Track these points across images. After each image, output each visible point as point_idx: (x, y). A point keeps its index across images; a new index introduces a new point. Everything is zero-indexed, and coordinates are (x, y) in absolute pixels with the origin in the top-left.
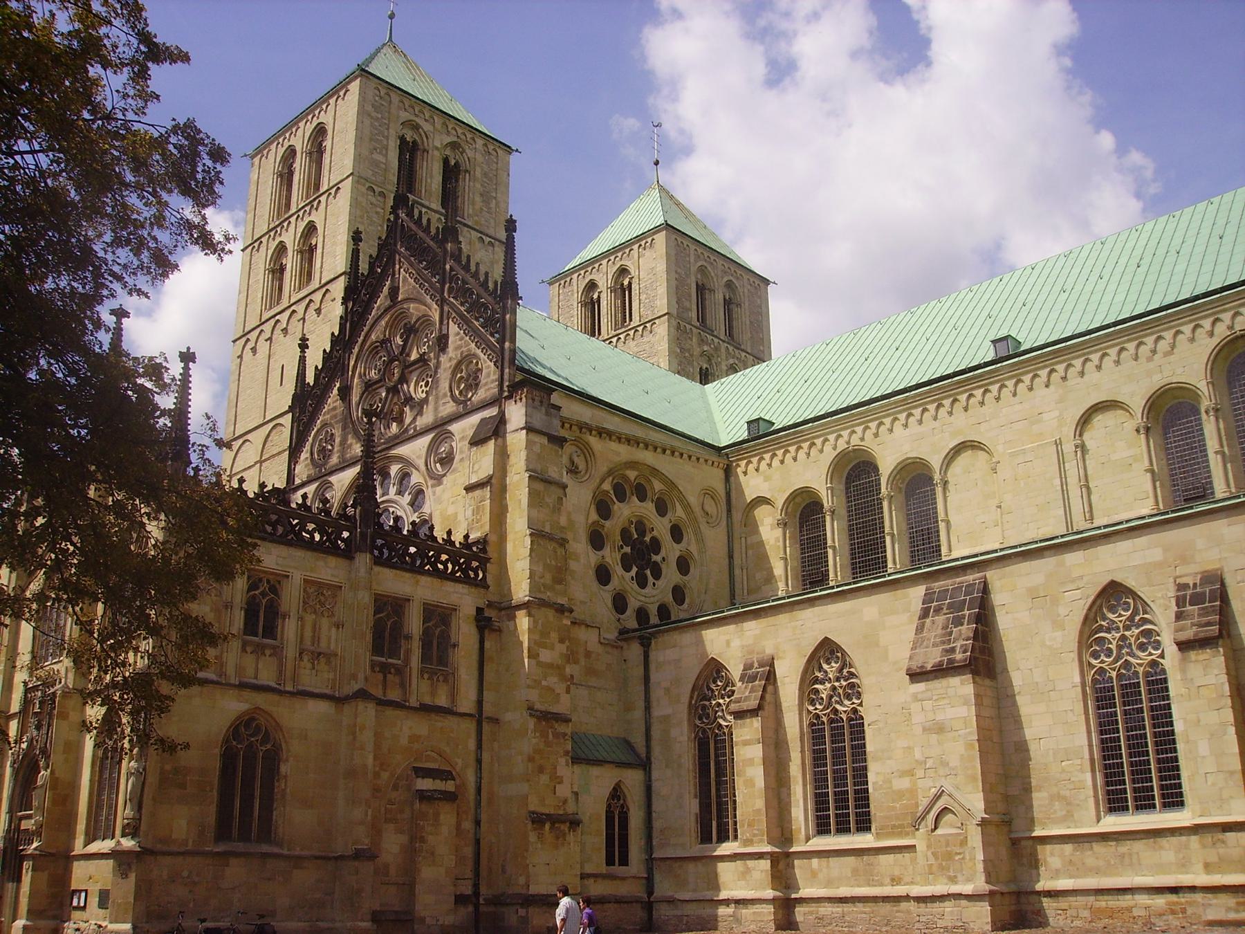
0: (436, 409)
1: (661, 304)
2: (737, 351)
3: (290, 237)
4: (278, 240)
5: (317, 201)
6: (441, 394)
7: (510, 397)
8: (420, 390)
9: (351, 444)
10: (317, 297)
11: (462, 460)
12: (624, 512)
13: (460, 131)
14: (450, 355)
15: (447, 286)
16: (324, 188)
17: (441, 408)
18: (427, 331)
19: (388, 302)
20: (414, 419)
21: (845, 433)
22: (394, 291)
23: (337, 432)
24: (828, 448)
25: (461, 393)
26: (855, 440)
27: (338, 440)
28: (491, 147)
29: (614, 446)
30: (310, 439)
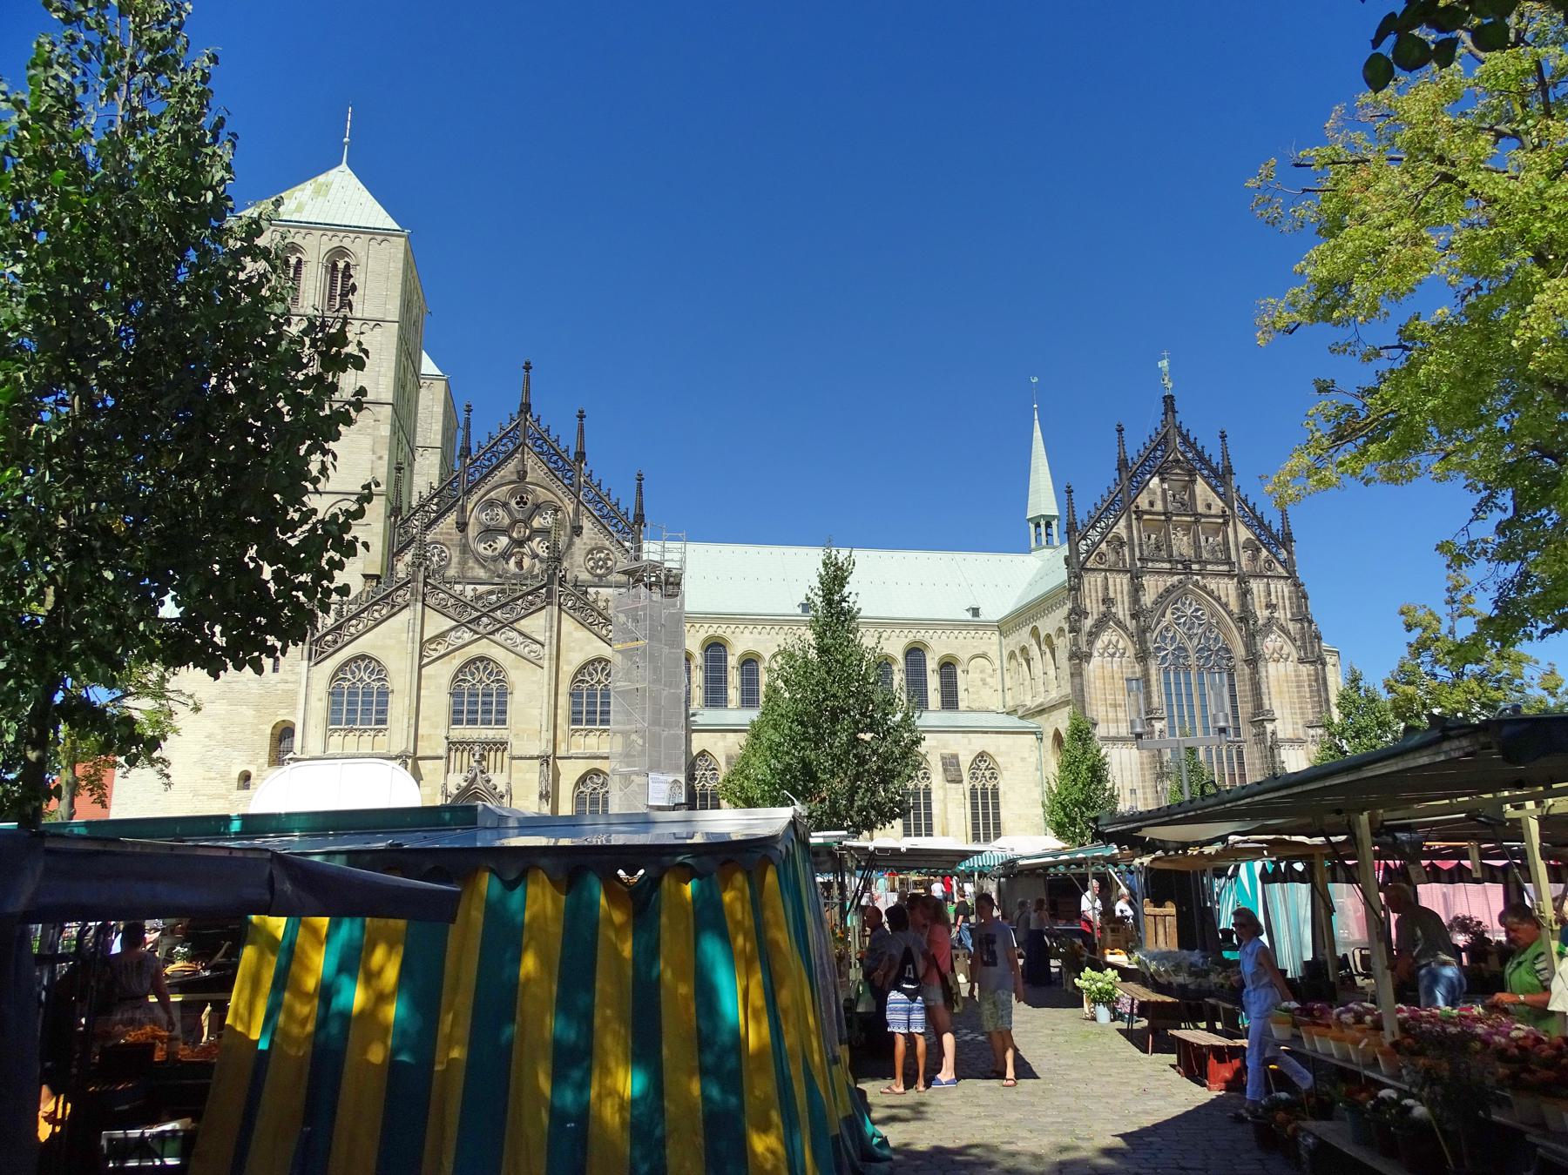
6: (576, 564)
9: (472, 568)
19: (514, 477)
21: (715, 626)
22: (522, 475)
24: (702, 631)
26: (720, 632)
27: (455, 560)
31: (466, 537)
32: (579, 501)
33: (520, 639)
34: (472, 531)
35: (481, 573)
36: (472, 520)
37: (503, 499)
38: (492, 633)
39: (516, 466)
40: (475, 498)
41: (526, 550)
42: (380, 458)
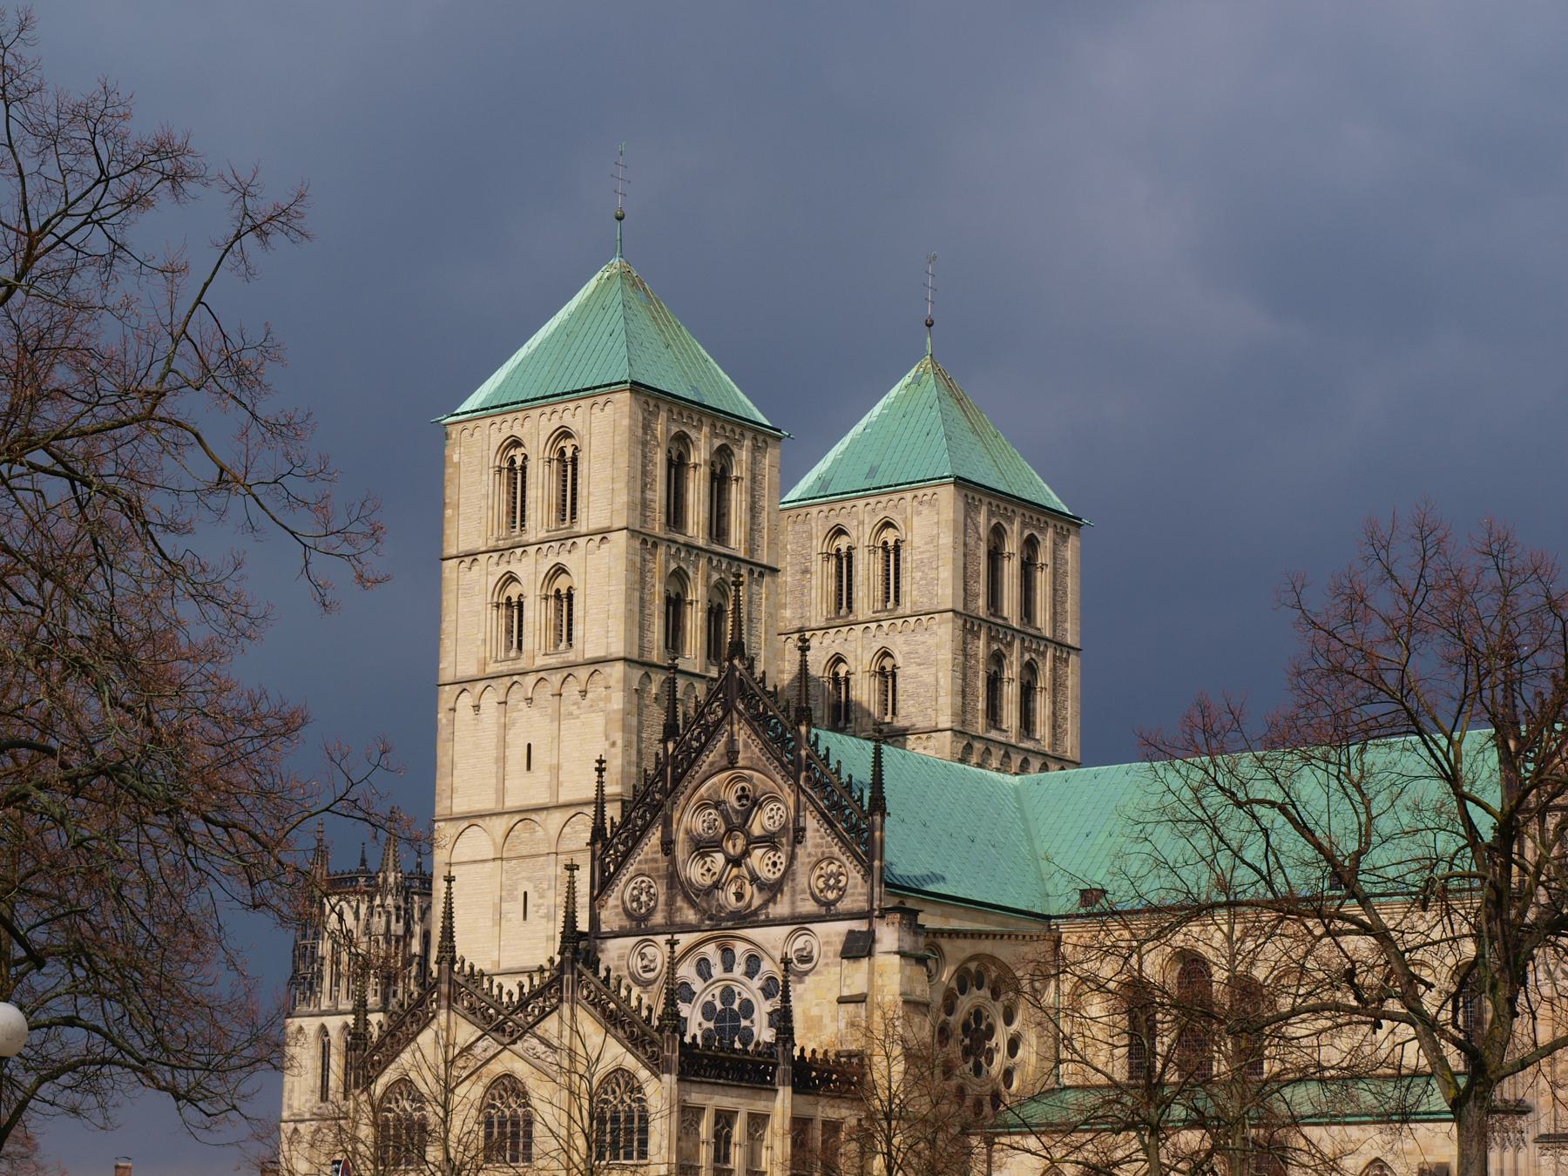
0: (793, 903)
1: (946, 592)
2: (1034, 641)
3: (530, 570)
4: (504, 568)
5: (571, 541)
6: (798, 888)
7: (882, 917)
8: (766, 869)
9: (680, 909)
10: (583, 673)
11: (827, 964)
12: (965, 1004)
13: (728, 428)
14: (810, 849)
15: (804, 774)
16: (582, 526)
17: (799, 903)
18: (772, 806)
19: (724, 762)
20: (765, 905)
22: (732, 754)
23: (660, 889)
25: (821, 891)
28: (760, 438)
29: (961, 943)
30: (621, 885)
31: (673, 862)
32: (799, 787)
33: (541, 1048)
34: (681, 851)
35: (690, 916)
36: (681, 837)
37: (716, 799)
38: (514, 1042)
39: (726, 744)
40: (682, 800)
41: (744, 870)
42: (613, 744)
